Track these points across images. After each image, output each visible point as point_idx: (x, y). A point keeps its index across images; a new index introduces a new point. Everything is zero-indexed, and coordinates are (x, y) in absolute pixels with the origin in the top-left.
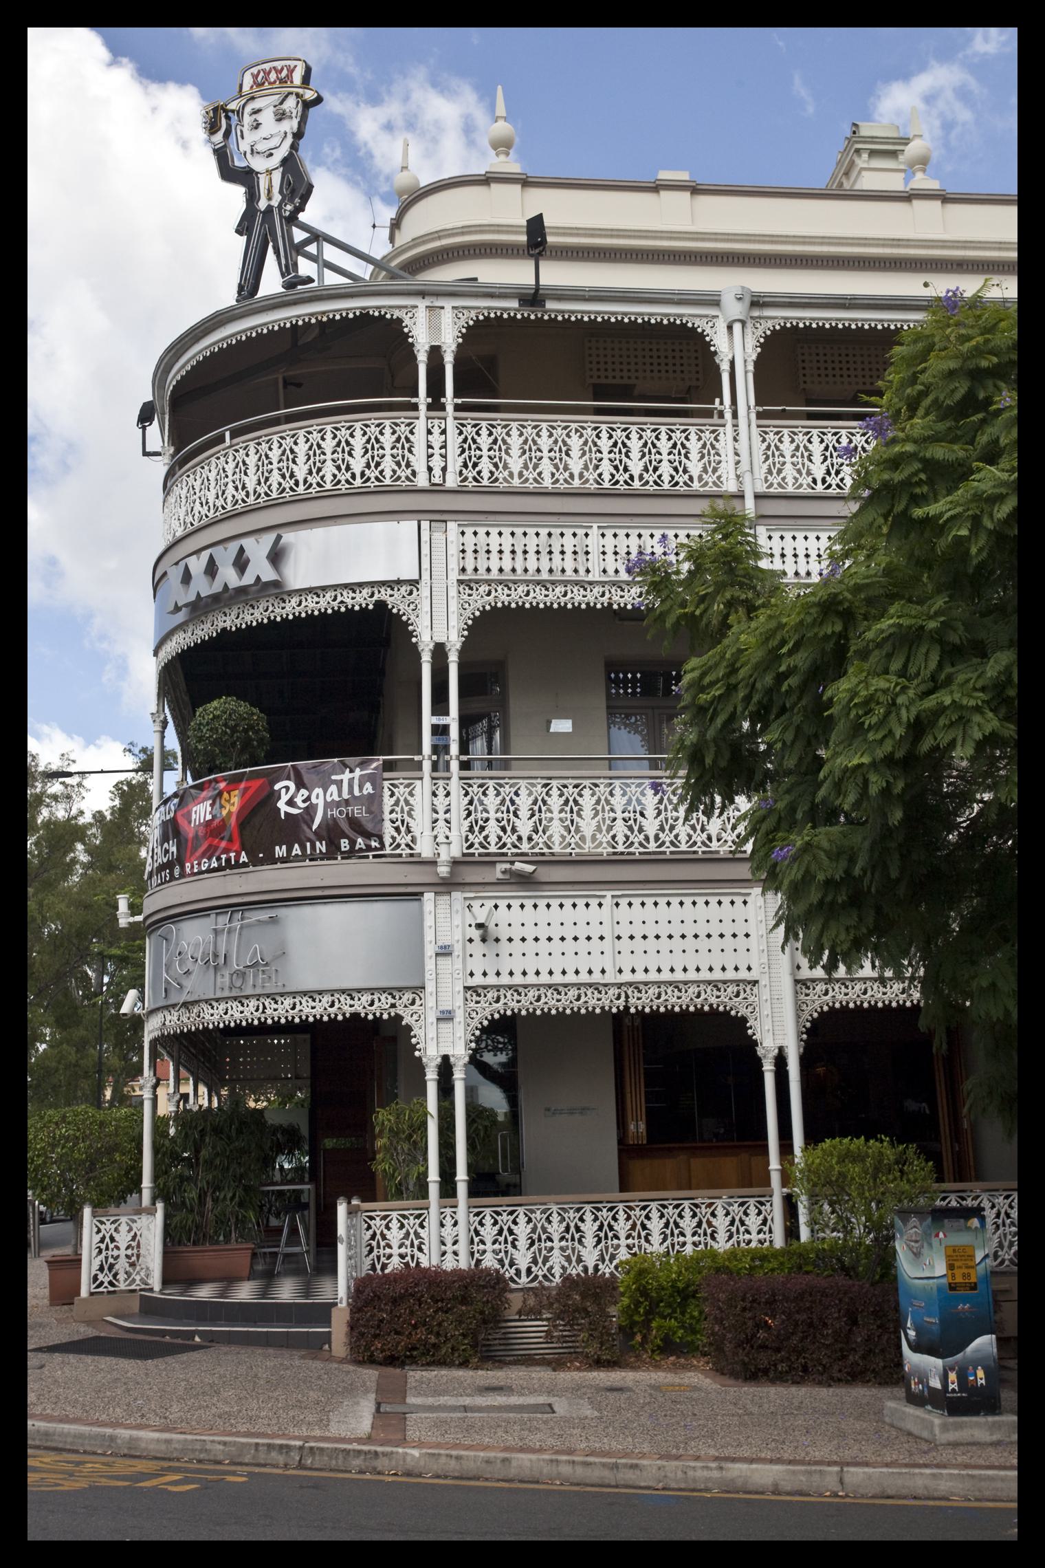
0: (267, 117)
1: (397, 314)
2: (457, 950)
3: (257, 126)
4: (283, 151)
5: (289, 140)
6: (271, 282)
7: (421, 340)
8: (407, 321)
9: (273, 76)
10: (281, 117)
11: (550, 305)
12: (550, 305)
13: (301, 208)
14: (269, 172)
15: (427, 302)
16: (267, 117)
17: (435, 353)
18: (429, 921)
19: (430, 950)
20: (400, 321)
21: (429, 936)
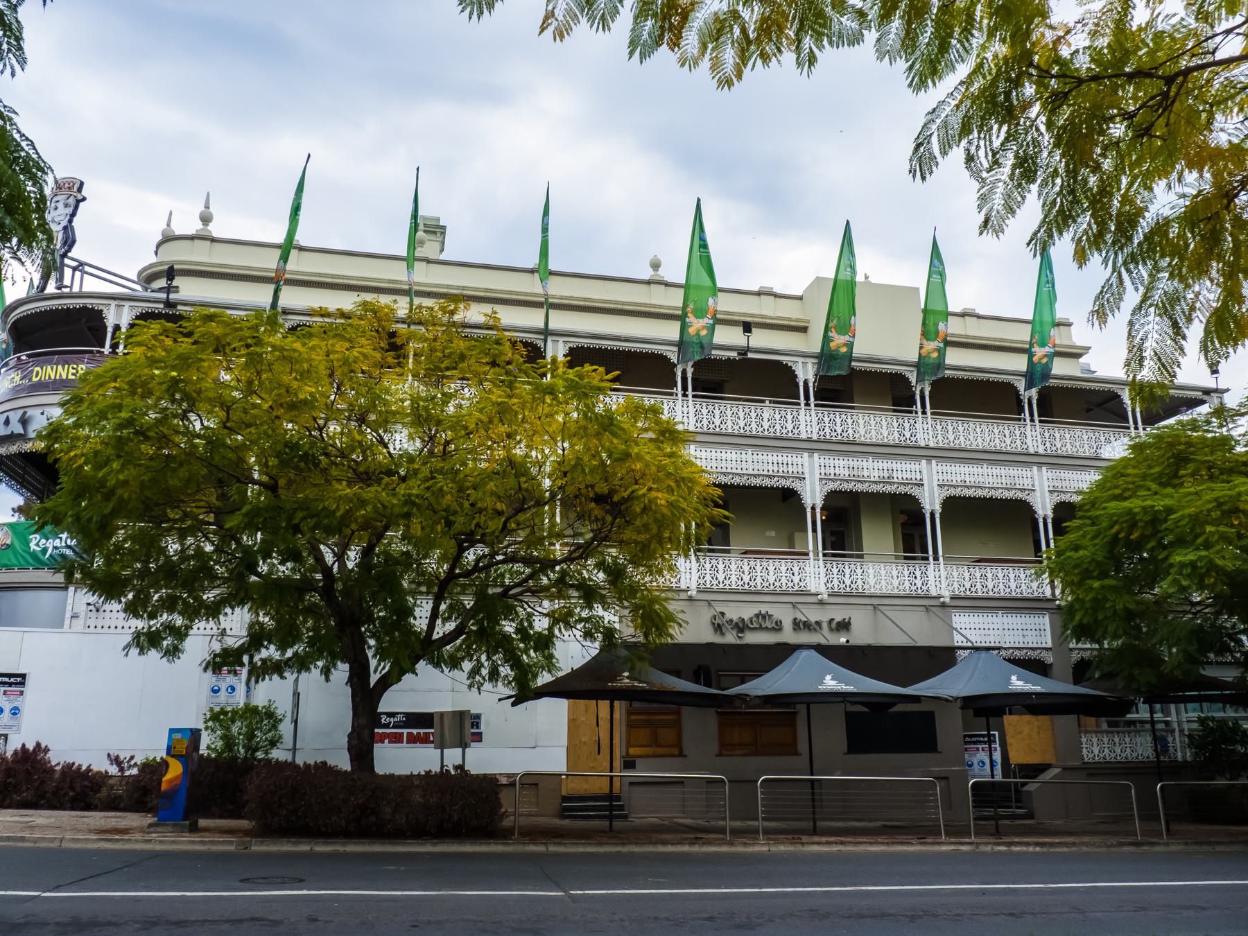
0: (60, 205)
1: (101, 308)
2: (82, 615)
3: (56, 209)
4: (64, 223)
5: (68, 217)
6: (51, 288)
7: (110, 321)
8: (105, 311)
9: (67, 185)
10: (66, 206)
11: (179, 307)
12: (179, 307)
13: (69, 250)
14: (58, 232)
15: (117, 302)
16: (60, 205)
17: (117, 328)
18: (70, 601)
19: (68, 615)
20: (102, 311)
21: (69, 608)
